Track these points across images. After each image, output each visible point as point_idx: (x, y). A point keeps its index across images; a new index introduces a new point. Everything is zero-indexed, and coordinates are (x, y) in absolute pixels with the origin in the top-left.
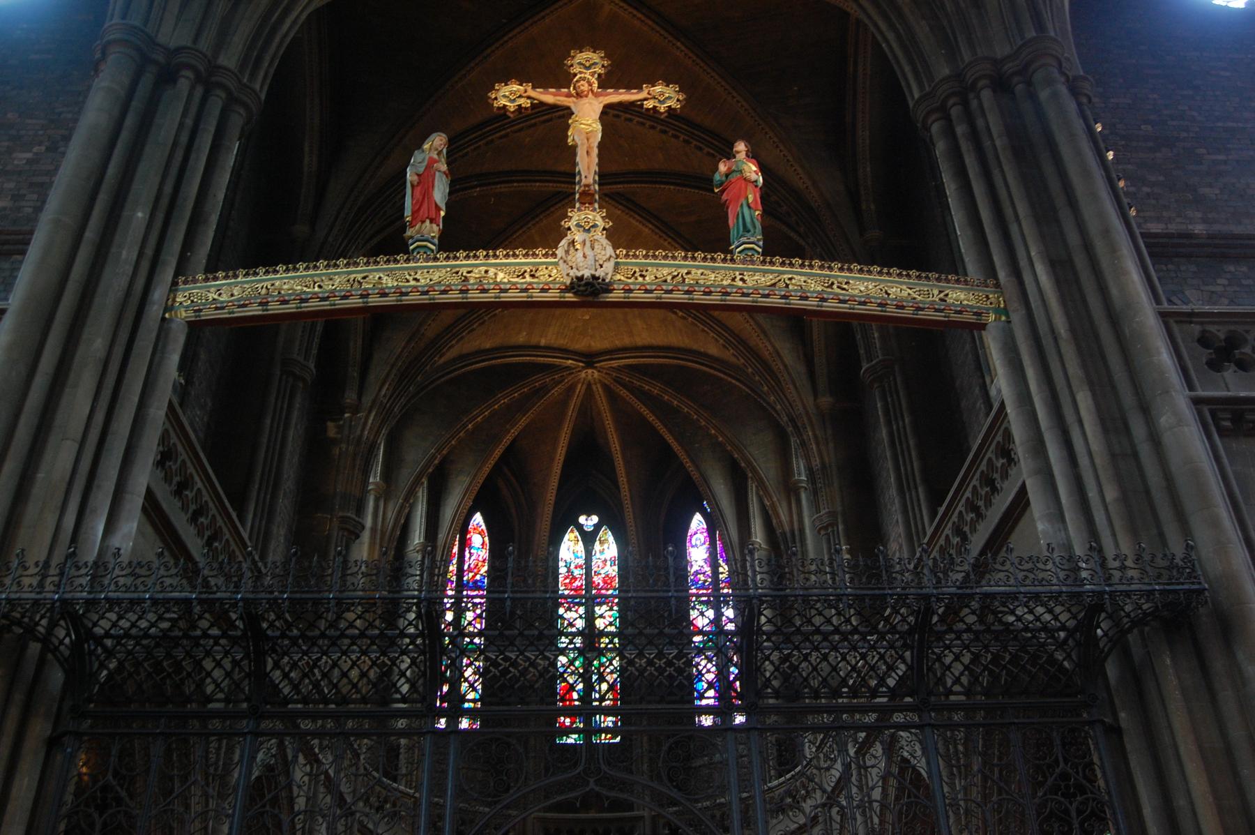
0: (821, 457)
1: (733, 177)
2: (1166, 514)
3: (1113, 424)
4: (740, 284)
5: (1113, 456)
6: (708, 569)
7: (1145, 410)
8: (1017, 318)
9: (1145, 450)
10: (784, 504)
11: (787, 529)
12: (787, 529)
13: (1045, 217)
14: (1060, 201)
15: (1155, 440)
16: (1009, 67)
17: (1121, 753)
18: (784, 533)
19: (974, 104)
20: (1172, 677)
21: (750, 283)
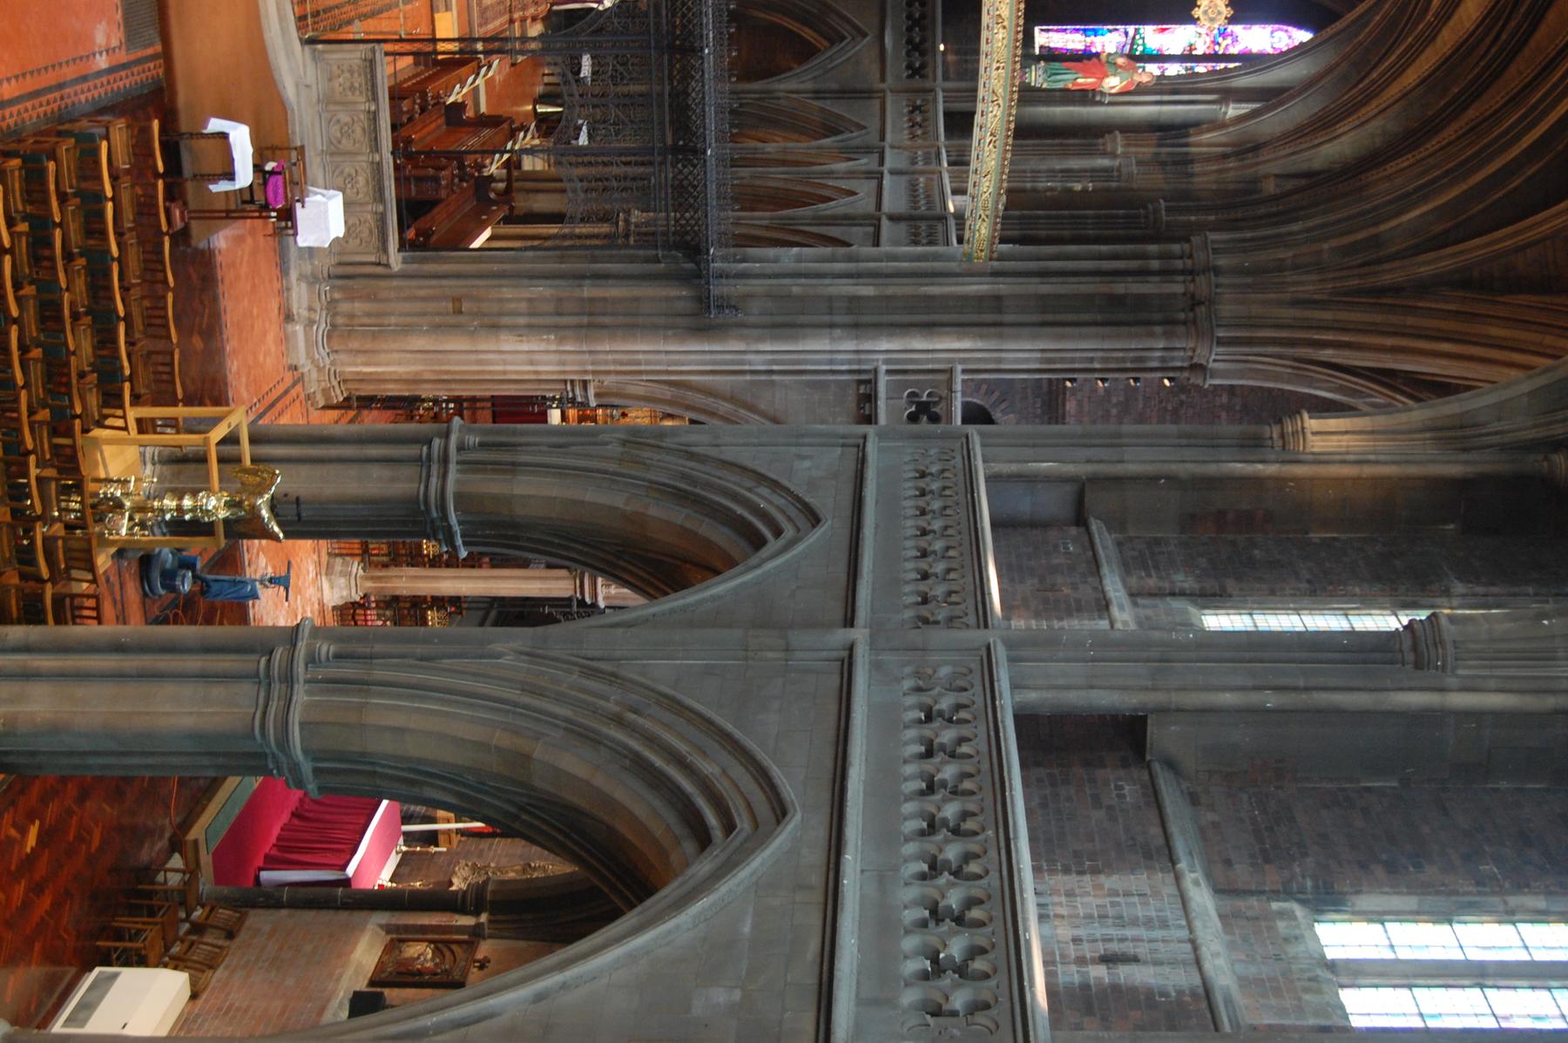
0: (1205, 174)
1: (1110, 70)
2: (779, 319)
3: (854, 304)
4: (995, 65)
5: (830, 299)
6: (1234, 50)
7: (856, 326)
8: (953, 266)
9: (827, 318)
10: (1224, 139)
11: (1192, 140)
12: (1192, 140)
13: (1045, 303)
14: (1049, 317)
15: (832, 326)
16: (1201, 311)
17: (647, 260)
18: (1187, 136)
19: (1181, 278)
20: (679, 293)
21: (995, 73)
